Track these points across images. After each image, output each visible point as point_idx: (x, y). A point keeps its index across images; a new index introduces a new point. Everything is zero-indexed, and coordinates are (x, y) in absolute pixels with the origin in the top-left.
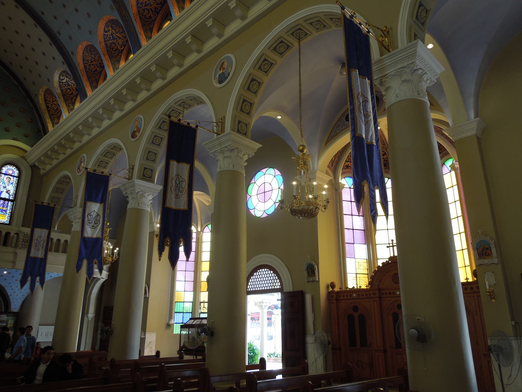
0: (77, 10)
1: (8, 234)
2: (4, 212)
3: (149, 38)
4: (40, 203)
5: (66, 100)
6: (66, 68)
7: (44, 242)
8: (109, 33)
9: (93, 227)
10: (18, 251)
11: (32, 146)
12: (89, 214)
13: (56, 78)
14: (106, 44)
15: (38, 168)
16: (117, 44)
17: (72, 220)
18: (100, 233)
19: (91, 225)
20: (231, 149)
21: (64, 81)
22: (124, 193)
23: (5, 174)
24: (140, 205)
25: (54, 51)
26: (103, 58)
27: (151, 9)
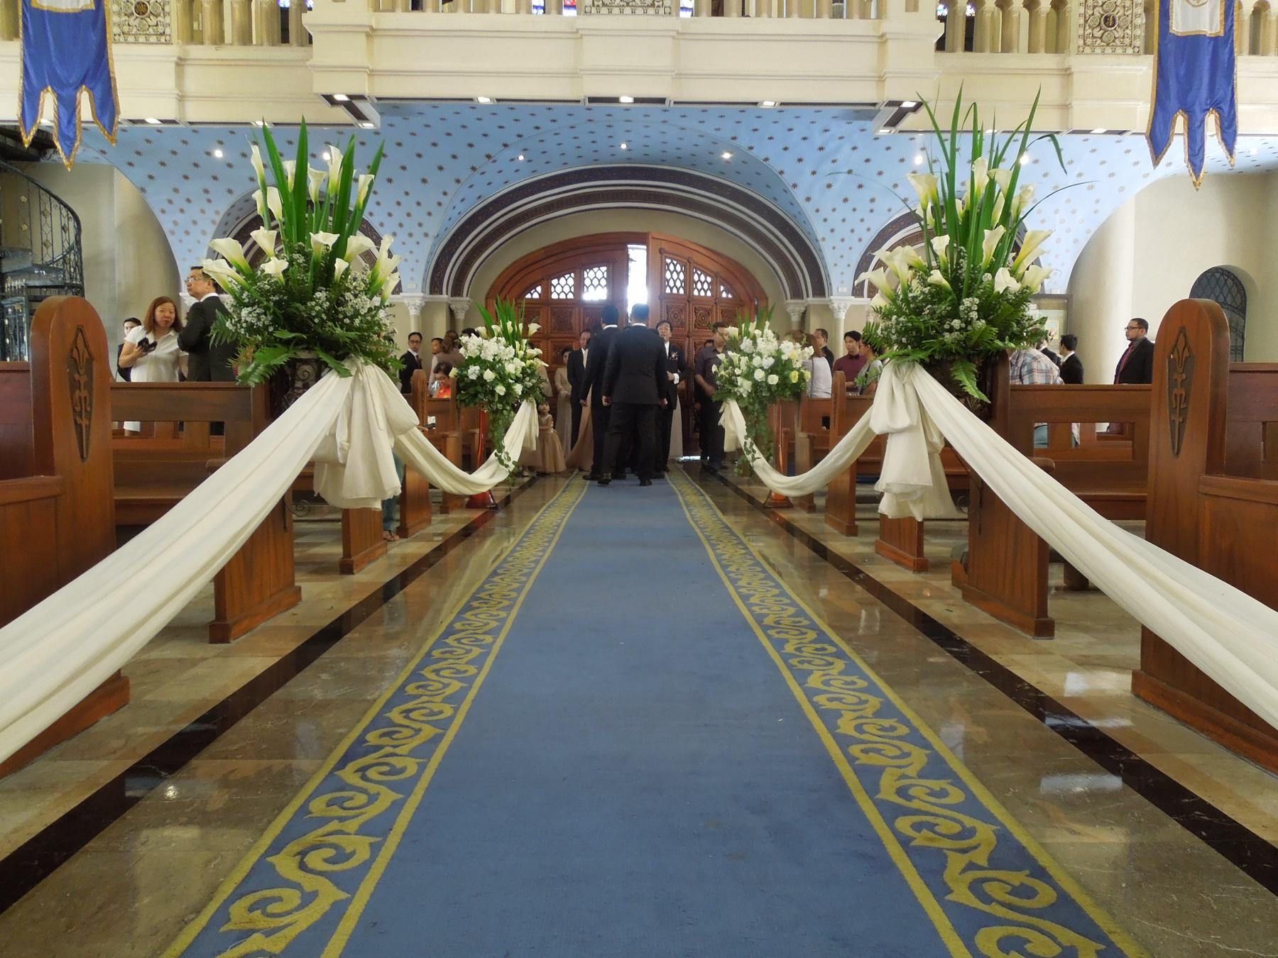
10: (1076, 62)
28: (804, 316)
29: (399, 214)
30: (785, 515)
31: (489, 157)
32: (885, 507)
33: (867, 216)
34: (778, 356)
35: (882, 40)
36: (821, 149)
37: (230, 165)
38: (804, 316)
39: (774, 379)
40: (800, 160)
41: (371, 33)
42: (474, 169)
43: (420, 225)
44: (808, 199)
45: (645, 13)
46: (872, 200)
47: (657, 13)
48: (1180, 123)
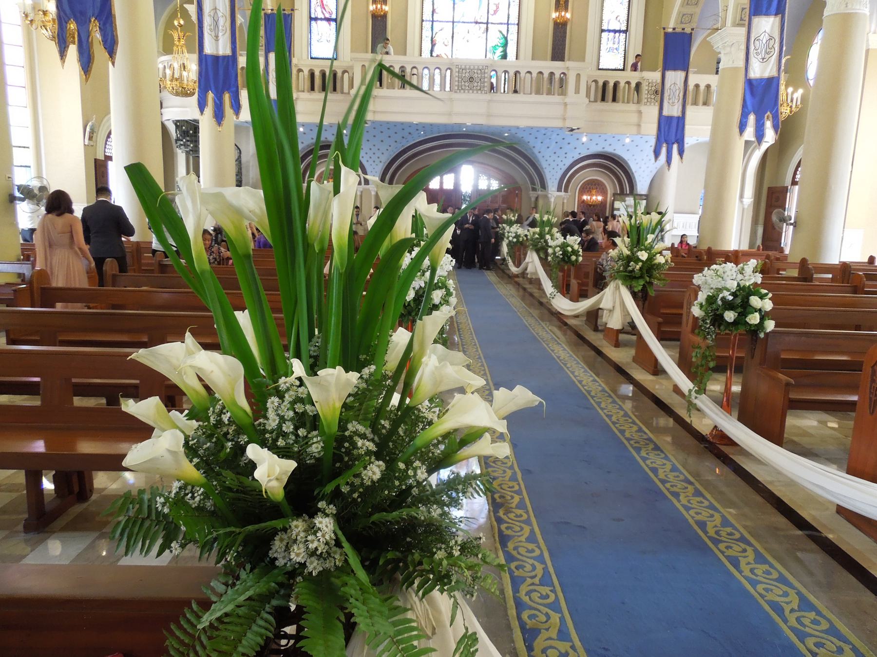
2: (615, 51)
4: (670, 30)
7: (680, 92)
9: (763, 59)
10: (643, 108)
12: (756, 39)
17: (718, 51)
18: (775, 69)
19: (760, 57)
24: (850, 6)
28: (537, 198)
29: (370, 153)
30: (516, 279)
31: (410, 133)
32: (529, 276)
33: (564, 160)
34: (516, 233)
35: (566, 104)
36: (545, 134)
37: (305, 133)
38: (537, 198)
39: (515, 240)
40: (536, 138)
42: (403, 137)
43: (378, 158)
44: (540, 152)
45: (477, 92)
46: (566, 153)
47: (481, 93)
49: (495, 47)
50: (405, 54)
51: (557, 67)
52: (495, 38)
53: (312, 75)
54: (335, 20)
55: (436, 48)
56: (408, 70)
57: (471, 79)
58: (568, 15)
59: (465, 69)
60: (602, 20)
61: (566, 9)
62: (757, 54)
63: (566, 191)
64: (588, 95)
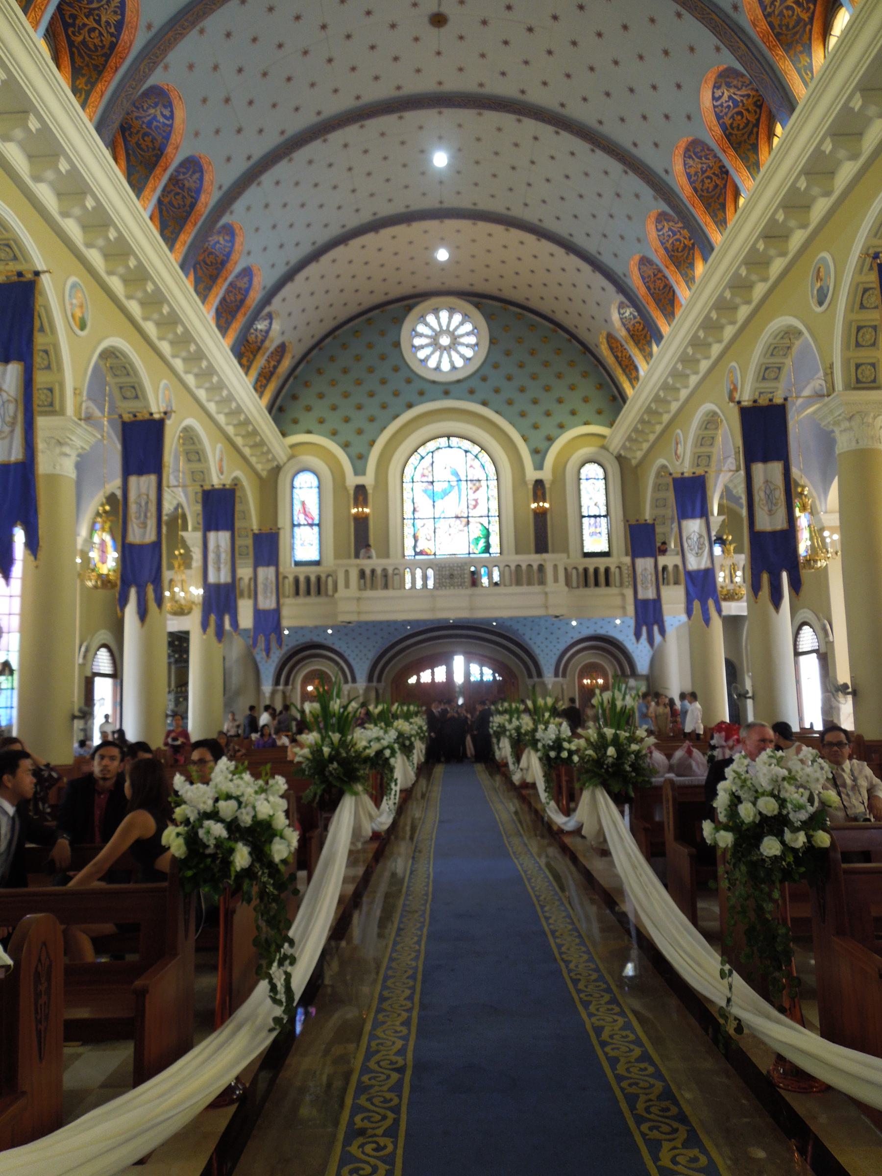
0: (611, 216)
1: (607, 570)
3: (721, 223)
5: (637, 343)
6: (621, 298)
8: (666, 229)
11: (611, 425)
12: (688, 538)
13: (615, 317)
14: (666, 249)
15: (625, 458)
16: (682, 239)
19: (694, 552)
20: (848, 416)
21: (627, 314)
22: (734, 492)
23: (587, 479)
25: (600, 280)
26: (667, 273)
27: (714, 174)
35: (546, 594)
38: (534, 687)
41: (359, 599)
48: (644, 629)
49: (477, 539)
50: (387, 556)
51: (535, 559)
52: (476, 530)
53: (297, 581)
54: (318, 525)
55: (419, 544)
56: (390, 571)
57: (452, 576)
58: (547, 505)
59: (445, 567)
60: (580, 507)
61: (544, 501)
62: (691, 550)
63: (564, 675)
64: (568, 583)
